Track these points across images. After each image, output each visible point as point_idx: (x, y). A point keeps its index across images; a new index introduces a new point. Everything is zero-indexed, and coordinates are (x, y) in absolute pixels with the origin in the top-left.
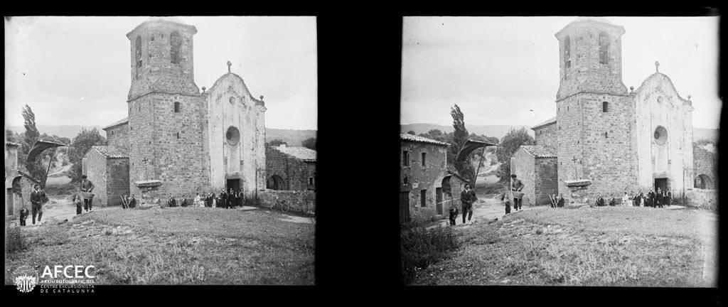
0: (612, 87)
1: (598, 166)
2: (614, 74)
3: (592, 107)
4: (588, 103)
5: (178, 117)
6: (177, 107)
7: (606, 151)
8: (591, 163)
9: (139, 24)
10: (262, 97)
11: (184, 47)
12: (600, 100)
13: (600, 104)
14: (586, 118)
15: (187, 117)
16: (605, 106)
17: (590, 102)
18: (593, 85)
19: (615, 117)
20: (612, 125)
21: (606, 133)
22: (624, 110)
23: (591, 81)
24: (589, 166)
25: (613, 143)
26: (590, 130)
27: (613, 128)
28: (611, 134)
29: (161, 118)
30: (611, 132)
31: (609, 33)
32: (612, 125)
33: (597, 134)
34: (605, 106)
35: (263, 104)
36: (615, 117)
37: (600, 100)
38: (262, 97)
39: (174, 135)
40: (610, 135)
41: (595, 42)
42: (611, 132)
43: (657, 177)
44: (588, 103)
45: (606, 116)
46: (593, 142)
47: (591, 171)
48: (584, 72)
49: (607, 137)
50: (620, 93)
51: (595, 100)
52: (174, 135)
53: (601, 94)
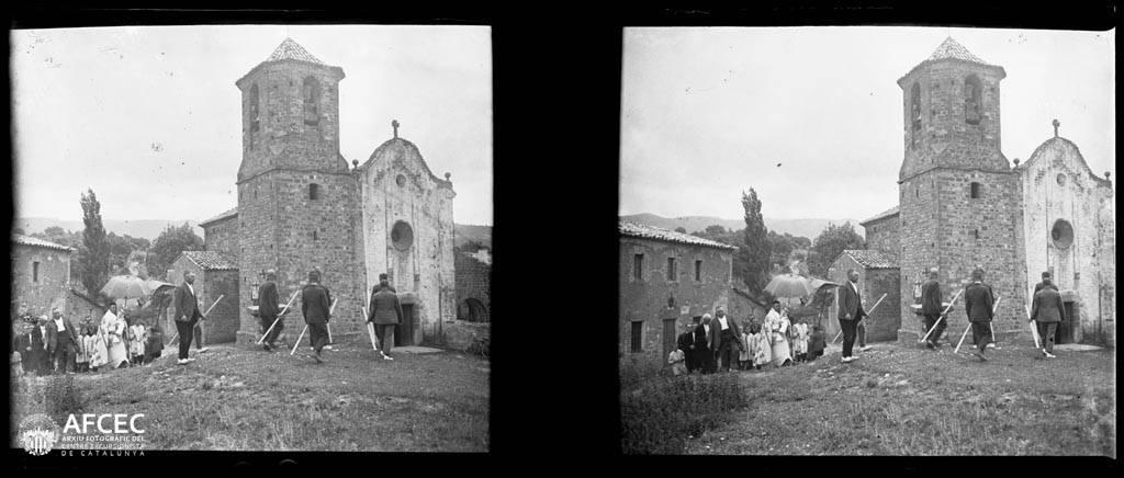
0: (985, 159)
2: (987, 140)
4: (947, 184)
5: (315, 206)
6: (313, 192)
8: (952, 277)
9: (254, 67)
10: (448, 175)
11: (325, 100)
12: (966, 180)
15: (329, 208)
16: (975, 190)
21: (977, 231)
23: (953, 151)
27: (986, 224)
29: (289, 208)
31: (981, 77)
33: (962, 233)
35: (449, 185)
37: (966, 180)
38: (448, 175)
39: (309, 234)
42: (984, 228)
44: (947, 184)
46: (956, 245)
48: (941, 137)
49: (977, 237)
51: (959, 180)
52: (309, 234)
53: (969, 171)
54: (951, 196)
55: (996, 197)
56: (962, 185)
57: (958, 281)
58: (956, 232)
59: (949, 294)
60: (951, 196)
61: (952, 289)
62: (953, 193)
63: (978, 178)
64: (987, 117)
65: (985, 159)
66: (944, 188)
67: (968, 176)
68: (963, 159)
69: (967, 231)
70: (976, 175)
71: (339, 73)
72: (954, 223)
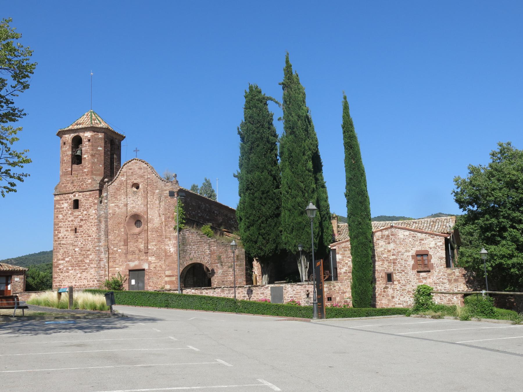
1: (67, 259)
3: (63, 206)
4: (59, 204)
7: (75, 246)
8: (60, 257)
12: (70, 199)
13: (71, 202)
14: (57, 217)
16: (76, 204)
17: (61, 202)
18: (65, 187)
19: (85, 212)
20: (82, 220)
21: (76, 229)
22: (95, 204)
23: (63, 184)
24: (59, 260)
25: (82, 237)
26: (61, 227)
27: (82, 223)
28: (81, 229)
30: (81, 226)
32: (82, 220)
34: (76, 204)
36: (85, 212)
37: (70, 199)
40: (79, 230)
41: (68, 147)
42: (81, 226)
43: (130, 269)
44: (59, 204)
45: (77, 213)
46: (63, 238)
47: (60, 264)
49: (76, 232)
50: (90, 189)
51: (66, 200)
53: (72, 193)
54: (61, 210)
55: (89, 207)
56: (67, 202)
57: (63, 259)
58: (62, 230)
59: (58, 267)
60: (61, 210)
61: (60, 264)
62: (63, 208)
63: (78, 196)
64: (85, 158)
65: (82, 185)
66: (57, 206)
67: (71, 196)
68: (70, 187)
69: (69, 229)
70: (77, 195)
71: (123, 138)
72: (62, 225)
